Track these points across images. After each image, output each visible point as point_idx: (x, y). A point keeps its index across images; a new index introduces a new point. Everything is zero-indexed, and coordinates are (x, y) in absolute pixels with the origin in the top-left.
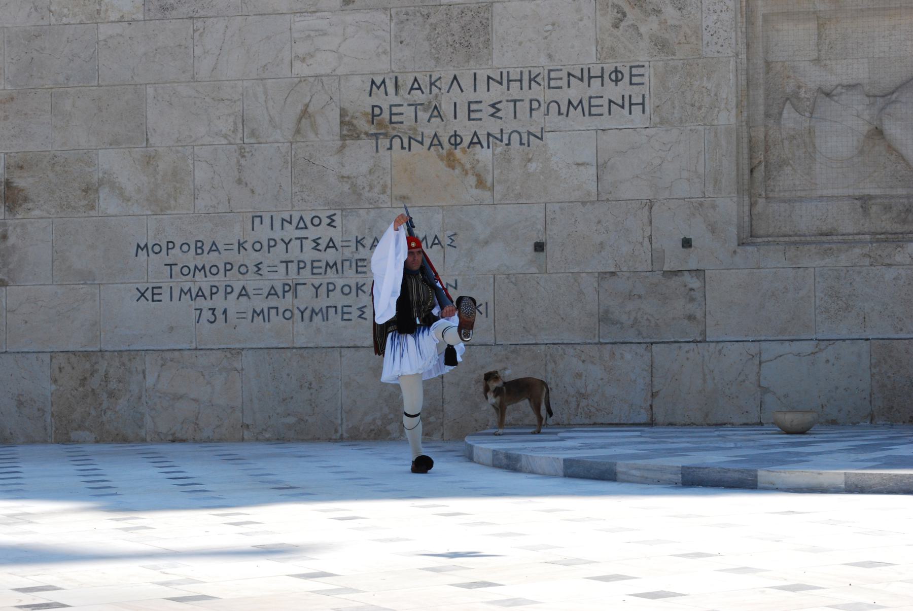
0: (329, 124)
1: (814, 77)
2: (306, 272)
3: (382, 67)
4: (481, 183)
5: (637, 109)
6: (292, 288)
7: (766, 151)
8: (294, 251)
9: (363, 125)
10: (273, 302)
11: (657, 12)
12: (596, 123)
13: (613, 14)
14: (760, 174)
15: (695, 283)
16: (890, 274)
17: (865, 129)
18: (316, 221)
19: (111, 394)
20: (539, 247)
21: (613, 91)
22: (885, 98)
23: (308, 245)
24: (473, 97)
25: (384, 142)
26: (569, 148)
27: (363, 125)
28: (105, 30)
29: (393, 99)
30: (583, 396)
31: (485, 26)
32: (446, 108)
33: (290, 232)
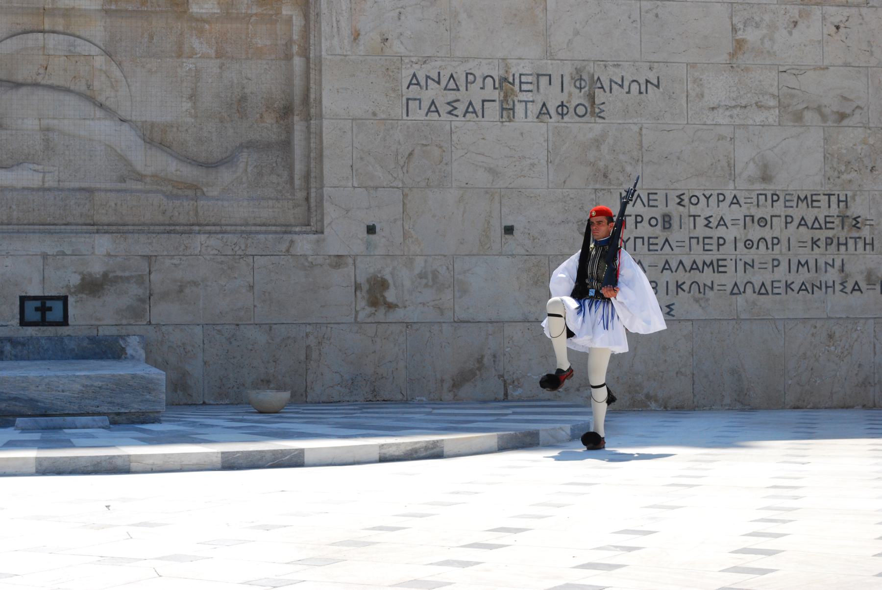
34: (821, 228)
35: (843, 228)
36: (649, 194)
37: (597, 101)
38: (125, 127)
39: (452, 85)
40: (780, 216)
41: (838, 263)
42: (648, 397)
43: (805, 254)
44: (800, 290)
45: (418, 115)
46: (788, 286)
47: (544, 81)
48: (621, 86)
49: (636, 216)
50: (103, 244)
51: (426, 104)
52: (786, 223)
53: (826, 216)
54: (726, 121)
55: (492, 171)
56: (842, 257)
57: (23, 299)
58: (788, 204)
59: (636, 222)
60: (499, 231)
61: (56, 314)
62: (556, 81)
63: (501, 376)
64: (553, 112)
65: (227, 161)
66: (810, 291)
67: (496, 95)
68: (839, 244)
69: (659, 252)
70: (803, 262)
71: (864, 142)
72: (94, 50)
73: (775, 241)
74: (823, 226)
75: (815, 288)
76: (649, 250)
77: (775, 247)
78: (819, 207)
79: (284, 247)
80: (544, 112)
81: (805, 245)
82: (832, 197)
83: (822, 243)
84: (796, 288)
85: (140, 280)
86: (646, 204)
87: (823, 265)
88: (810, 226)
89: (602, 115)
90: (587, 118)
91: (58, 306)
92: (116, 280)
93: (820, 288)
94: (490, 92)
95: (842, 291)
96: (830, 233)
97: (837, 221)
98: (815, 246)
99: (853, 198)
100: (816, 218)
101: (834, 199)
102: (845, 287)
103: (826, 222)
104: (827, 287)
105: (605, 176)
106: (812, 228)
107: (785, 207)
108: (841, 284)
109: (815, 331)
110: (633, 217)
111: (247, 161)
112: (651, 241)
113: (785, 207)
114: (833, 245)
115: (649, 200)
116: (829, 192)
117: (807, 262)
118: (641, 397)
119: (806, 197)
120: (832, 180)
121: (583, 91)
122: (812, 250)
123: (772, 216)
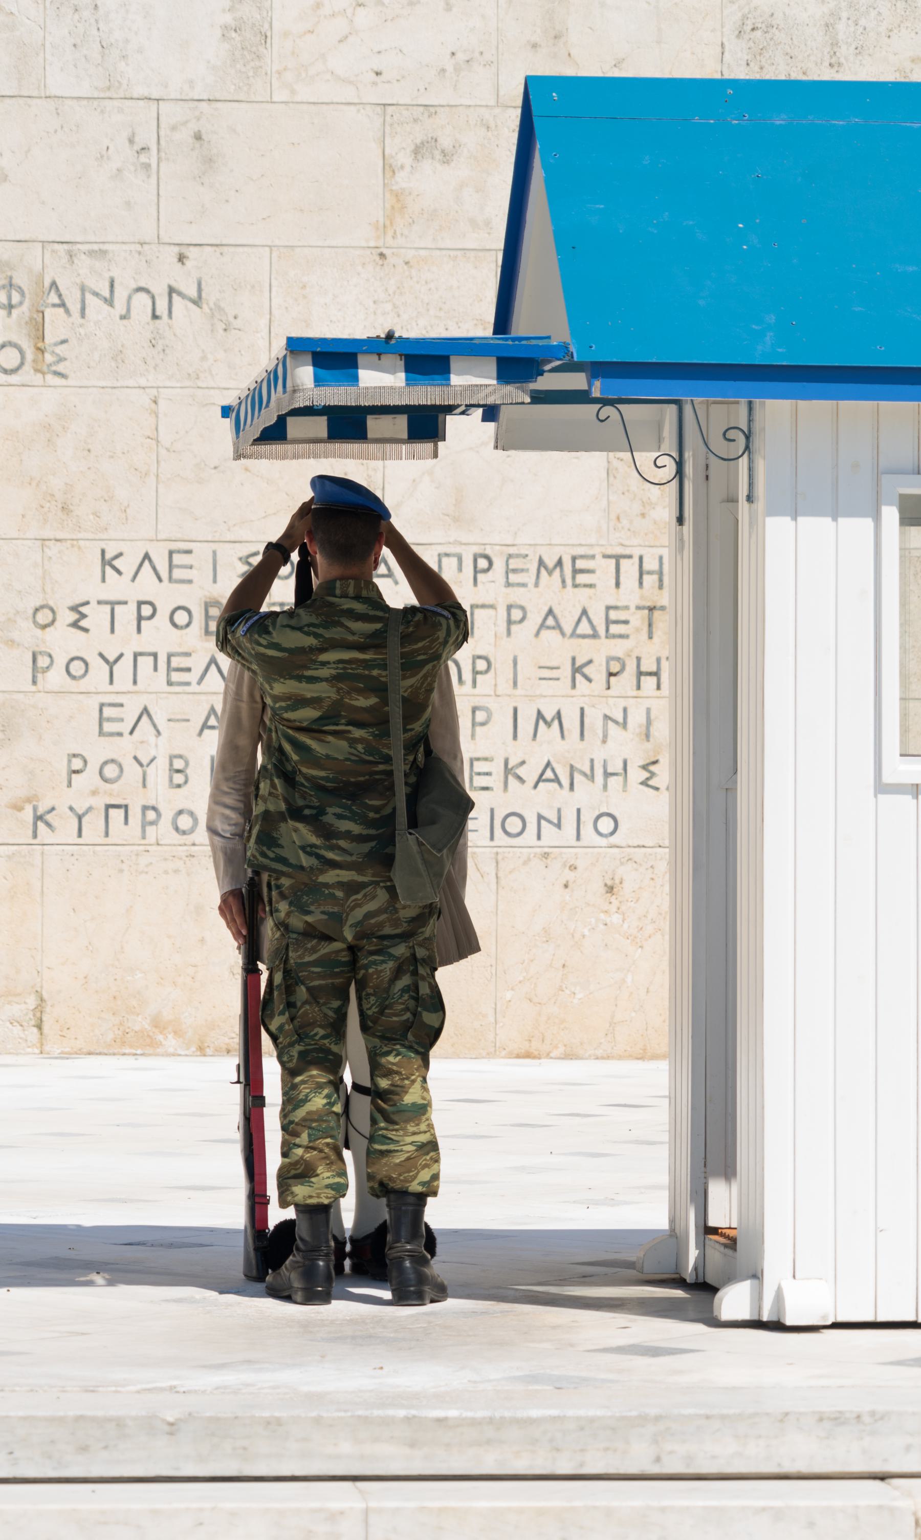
34: (595, 636)
35: (650, 637)
36: (171, 553)
37: (50, 338)
40: (492, 607)
41: (637, 718)
42: (158, 1024)
43: (556, 697)
44: (540, 779)
46: (508, 770)
48: (110, 302)
49: (140, 604)
52: (510, 622)
53: (608, 608)
56: (647, 703)
58: (513, 578)
59: (140, 618)
66: (565, 782)
68: (640, 674)
69: (194, 688)
70: (549, 715)
73: (481, 665)
74: (602, 630)
75: (578, 778)
76: (170, 683)
77: (479, 678)
78: (591, 586)
81: (554, 674)
82: (624, 563)
83: (597, 672)
84: (531, 778)
86: (164, 575)
87: (600, 722)
88: (568, 629)
89: (60, 368)
90: (27, 374)
93: (591, 778)
95: (644, 783)
96: (618, 648)
97: (638, 619)
98: (578, 677)
100: (584, 612)
101: (629, 568)
102: (653, 774)
103: (608, 622)
104: (607, 775)
105: (65, 509)
106: (574, 634)
107: (508, 584)
108: (645, 767)
109: (569, 875)
110: (133, 607)
112: (176, 662)
113: (508, 584)
114: (625, 675)
115: (171, 567)
116: (619, 551)
117: (559, 715)
118: (140, 1023)
119: (560, 563)
120: (625, 522)
121: (15, 312)
122: (574, 686)
123: (472, 607)
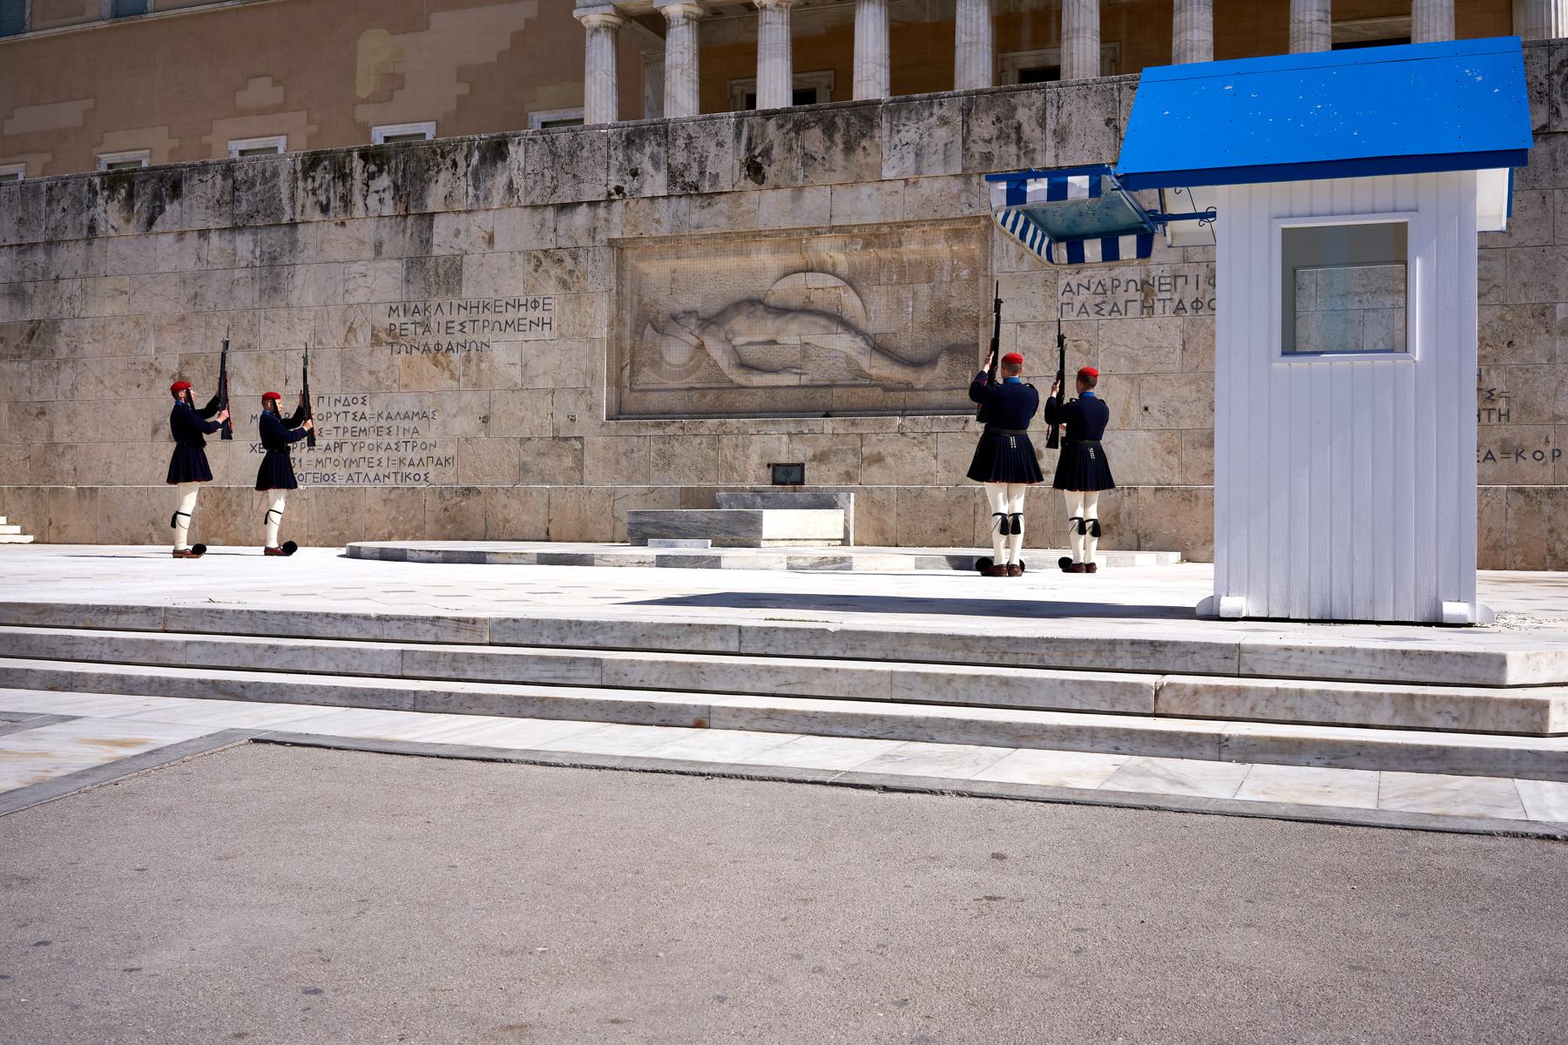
0: (363, 337)
1: (668, 303)
2: (348, 435)
3: (396, 296)
4: (452, 376)
5: (547, 327)
6: (339, 446)
7: (633, 356)
8: (341, 423)
9: (383, 336)
10: (328, 454)
11: (560, 261)
12: (521, 336)
13: (534, 262)
14: (627, 372)
15: (577, 445)
16: (697, 441)
17: (695, 341)
18: (355, 401)
19: (234, 515)
20: (485, 420)
21: (534, 315)
22: (712, 321)
23: (350, 416)
24: (449, 318)
25: (396, 348)
26: (503, 355)
27: (383, 336)
28: (238, 274)
29: (403, 320)
30: (506, 520)
31: (459, 270)
32: (434, 326)
33: (340, 408)
38: (858, 339)
39: (1100, 290)
45: (1073, 316)
47: (1180, 281)
50: (829, 425)
51: (1077, 306)
54: (1356, 305)
55: (1135, 360)
57: (775, 467)
60: (1135, 411)
61: (795, 476)
62: (1192, 281)
63: (1135, 531)
64: (1188, 307)
65: (931, 362)
67: (1139, 296)
71: (1502, 318)
72: (840, 283)
79: (961, 425)
80: (1179, 309)
85: (855, 452)
91: (797, 470)
92: (836, 453)
94: (1133, 294)
99: (1488, 372)
111: (943, 363)
